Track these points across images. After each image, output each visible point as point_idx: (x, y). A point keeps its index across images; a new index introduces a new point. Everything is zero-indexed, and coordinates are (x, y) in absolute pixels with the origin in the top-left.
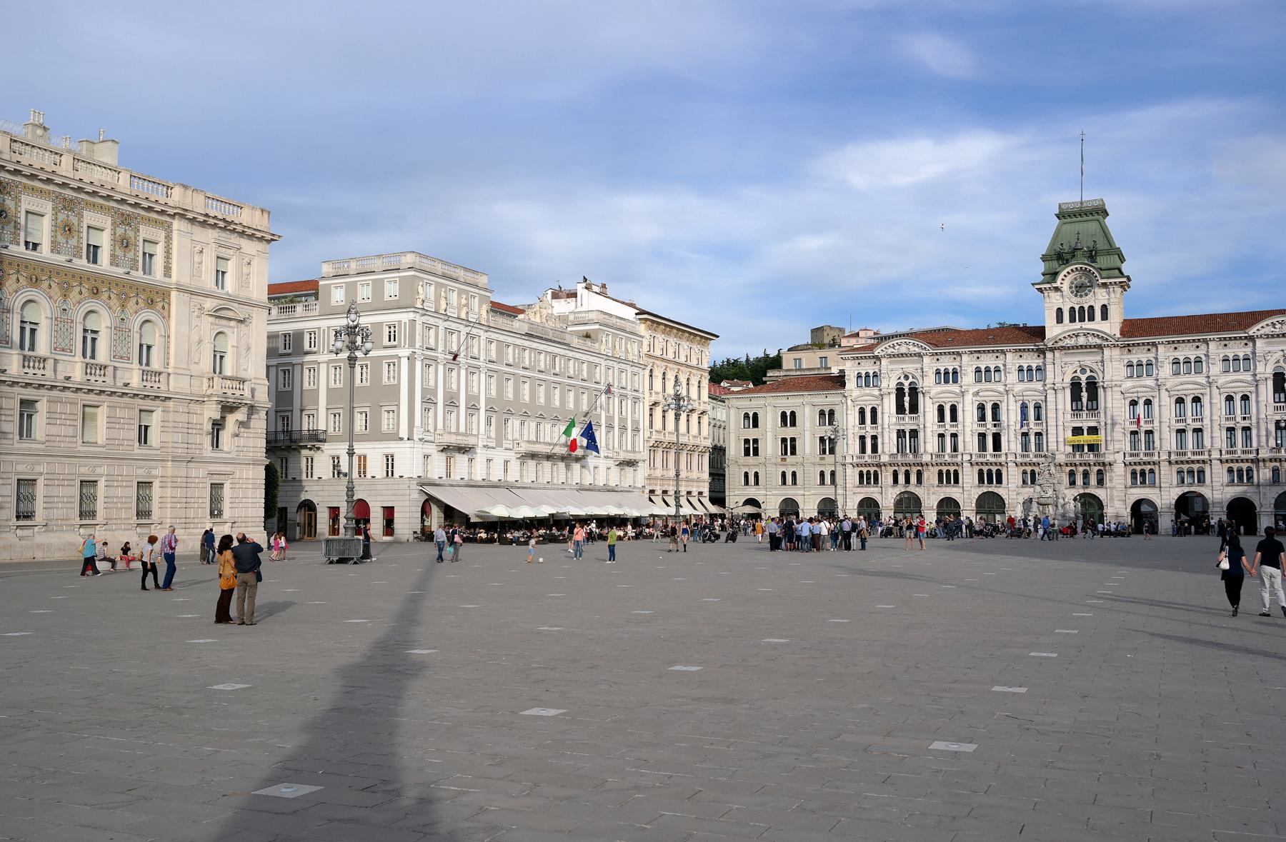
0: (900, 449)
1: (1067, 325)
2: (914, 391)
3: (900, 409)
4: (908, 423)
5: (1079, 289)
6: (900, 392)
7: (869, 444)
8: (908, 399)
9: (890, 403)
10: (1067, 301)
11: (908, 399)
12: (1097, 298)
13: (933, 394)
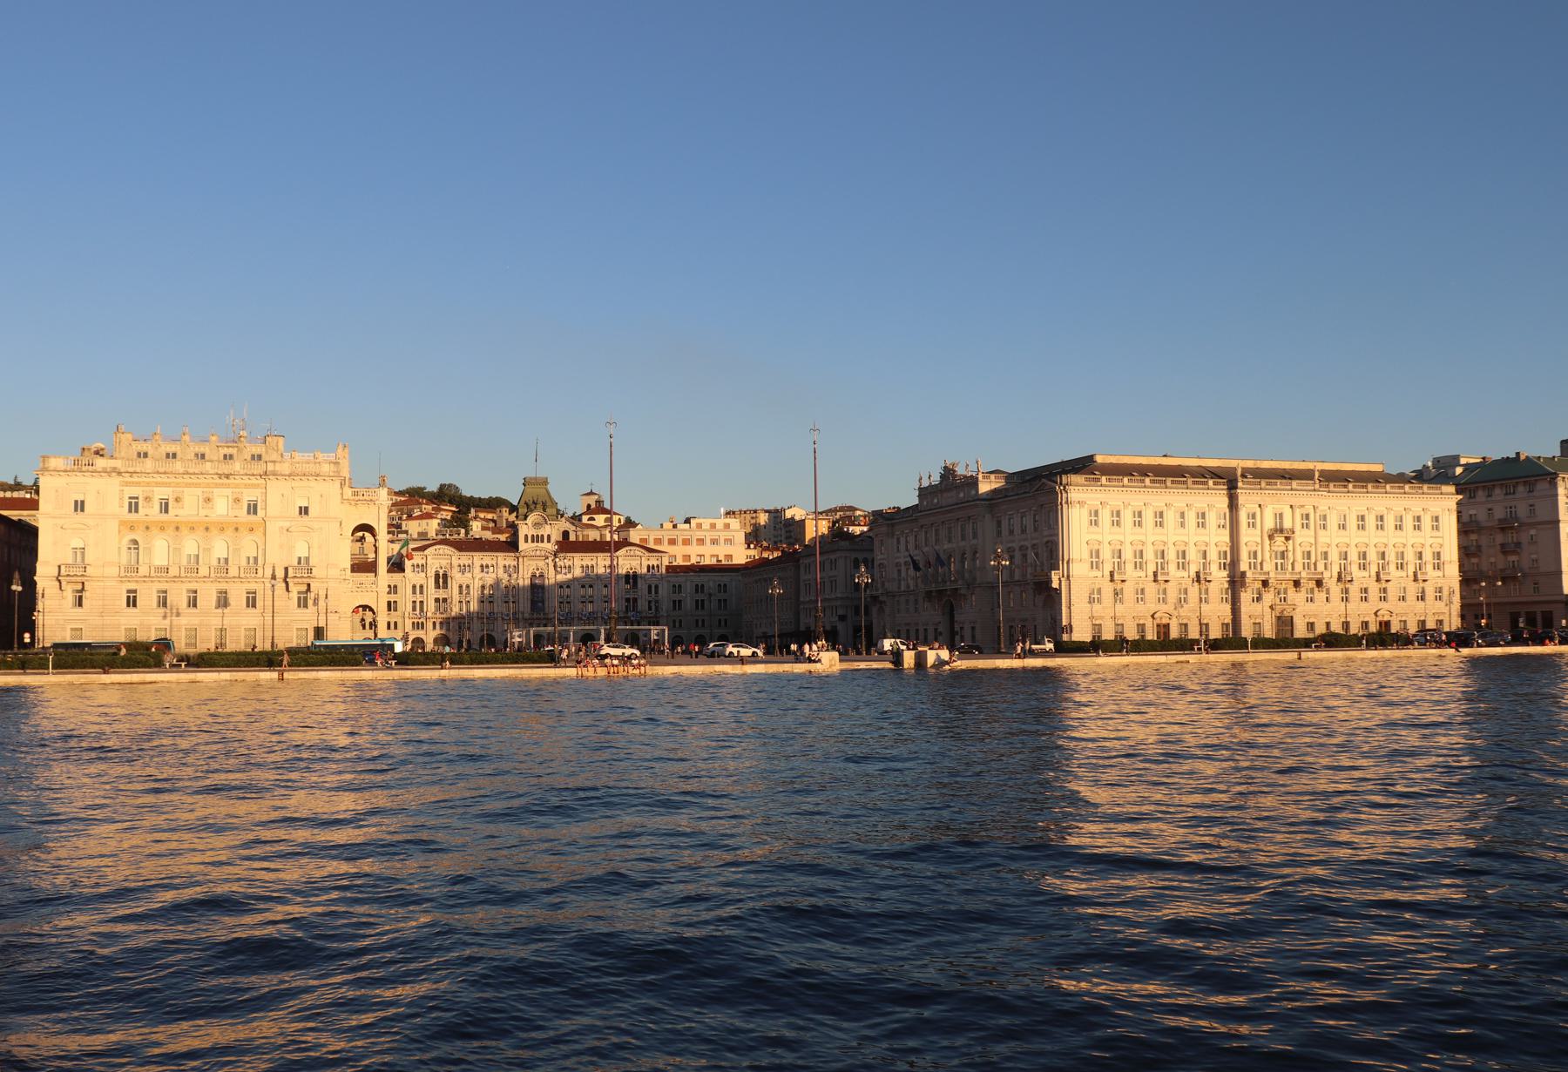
0: (438, 609)
1: (530, 545)
2: (445, 576)
3: (437, 586)
4: (441, 594)
5: (537, 525)
6: (437, 576)
7: (419, 606)
8: (442, 580)
9: (432, 581)
10: (532, 532)
11: (442, 580)
12: (546, 530)
13: (457, 578)
